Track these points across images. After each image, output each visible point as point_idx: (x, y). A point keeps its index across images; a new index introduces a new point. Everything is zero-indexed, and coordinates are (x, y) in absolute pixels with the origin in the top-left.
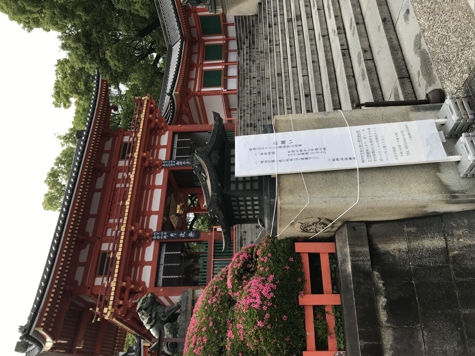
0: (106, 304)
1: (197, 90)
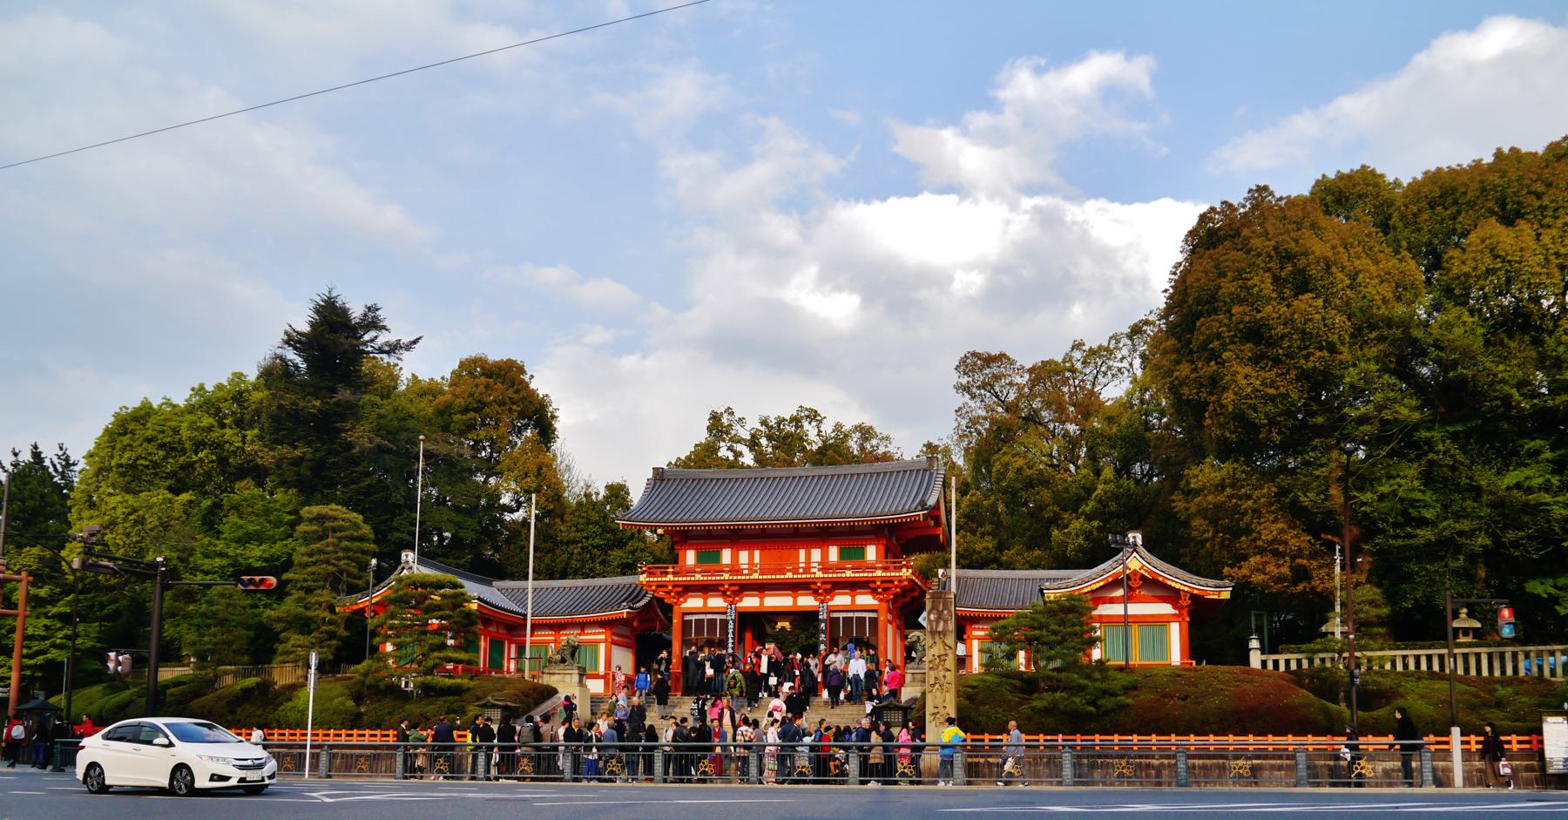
0: (651, 574)
1: (975, 633)
